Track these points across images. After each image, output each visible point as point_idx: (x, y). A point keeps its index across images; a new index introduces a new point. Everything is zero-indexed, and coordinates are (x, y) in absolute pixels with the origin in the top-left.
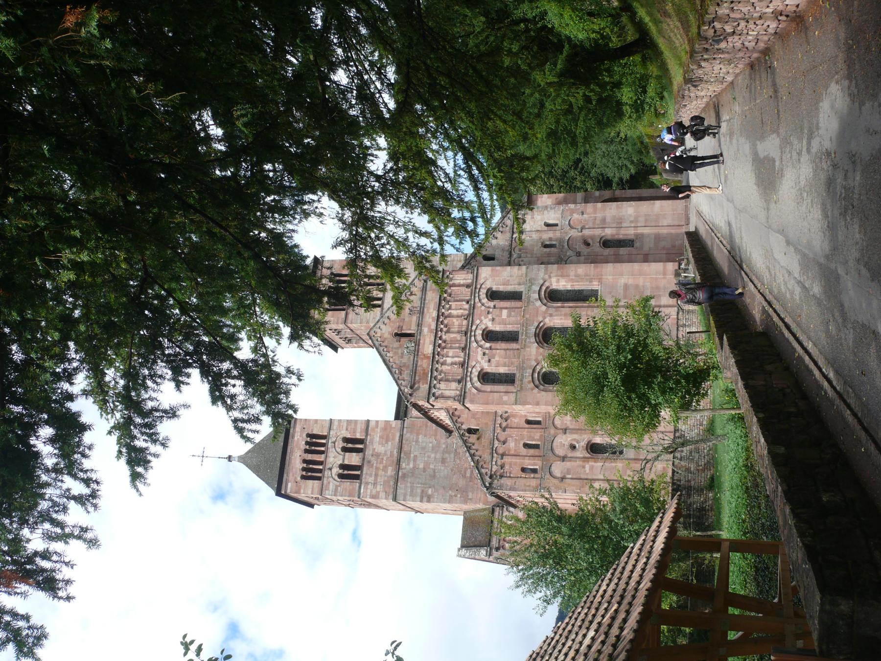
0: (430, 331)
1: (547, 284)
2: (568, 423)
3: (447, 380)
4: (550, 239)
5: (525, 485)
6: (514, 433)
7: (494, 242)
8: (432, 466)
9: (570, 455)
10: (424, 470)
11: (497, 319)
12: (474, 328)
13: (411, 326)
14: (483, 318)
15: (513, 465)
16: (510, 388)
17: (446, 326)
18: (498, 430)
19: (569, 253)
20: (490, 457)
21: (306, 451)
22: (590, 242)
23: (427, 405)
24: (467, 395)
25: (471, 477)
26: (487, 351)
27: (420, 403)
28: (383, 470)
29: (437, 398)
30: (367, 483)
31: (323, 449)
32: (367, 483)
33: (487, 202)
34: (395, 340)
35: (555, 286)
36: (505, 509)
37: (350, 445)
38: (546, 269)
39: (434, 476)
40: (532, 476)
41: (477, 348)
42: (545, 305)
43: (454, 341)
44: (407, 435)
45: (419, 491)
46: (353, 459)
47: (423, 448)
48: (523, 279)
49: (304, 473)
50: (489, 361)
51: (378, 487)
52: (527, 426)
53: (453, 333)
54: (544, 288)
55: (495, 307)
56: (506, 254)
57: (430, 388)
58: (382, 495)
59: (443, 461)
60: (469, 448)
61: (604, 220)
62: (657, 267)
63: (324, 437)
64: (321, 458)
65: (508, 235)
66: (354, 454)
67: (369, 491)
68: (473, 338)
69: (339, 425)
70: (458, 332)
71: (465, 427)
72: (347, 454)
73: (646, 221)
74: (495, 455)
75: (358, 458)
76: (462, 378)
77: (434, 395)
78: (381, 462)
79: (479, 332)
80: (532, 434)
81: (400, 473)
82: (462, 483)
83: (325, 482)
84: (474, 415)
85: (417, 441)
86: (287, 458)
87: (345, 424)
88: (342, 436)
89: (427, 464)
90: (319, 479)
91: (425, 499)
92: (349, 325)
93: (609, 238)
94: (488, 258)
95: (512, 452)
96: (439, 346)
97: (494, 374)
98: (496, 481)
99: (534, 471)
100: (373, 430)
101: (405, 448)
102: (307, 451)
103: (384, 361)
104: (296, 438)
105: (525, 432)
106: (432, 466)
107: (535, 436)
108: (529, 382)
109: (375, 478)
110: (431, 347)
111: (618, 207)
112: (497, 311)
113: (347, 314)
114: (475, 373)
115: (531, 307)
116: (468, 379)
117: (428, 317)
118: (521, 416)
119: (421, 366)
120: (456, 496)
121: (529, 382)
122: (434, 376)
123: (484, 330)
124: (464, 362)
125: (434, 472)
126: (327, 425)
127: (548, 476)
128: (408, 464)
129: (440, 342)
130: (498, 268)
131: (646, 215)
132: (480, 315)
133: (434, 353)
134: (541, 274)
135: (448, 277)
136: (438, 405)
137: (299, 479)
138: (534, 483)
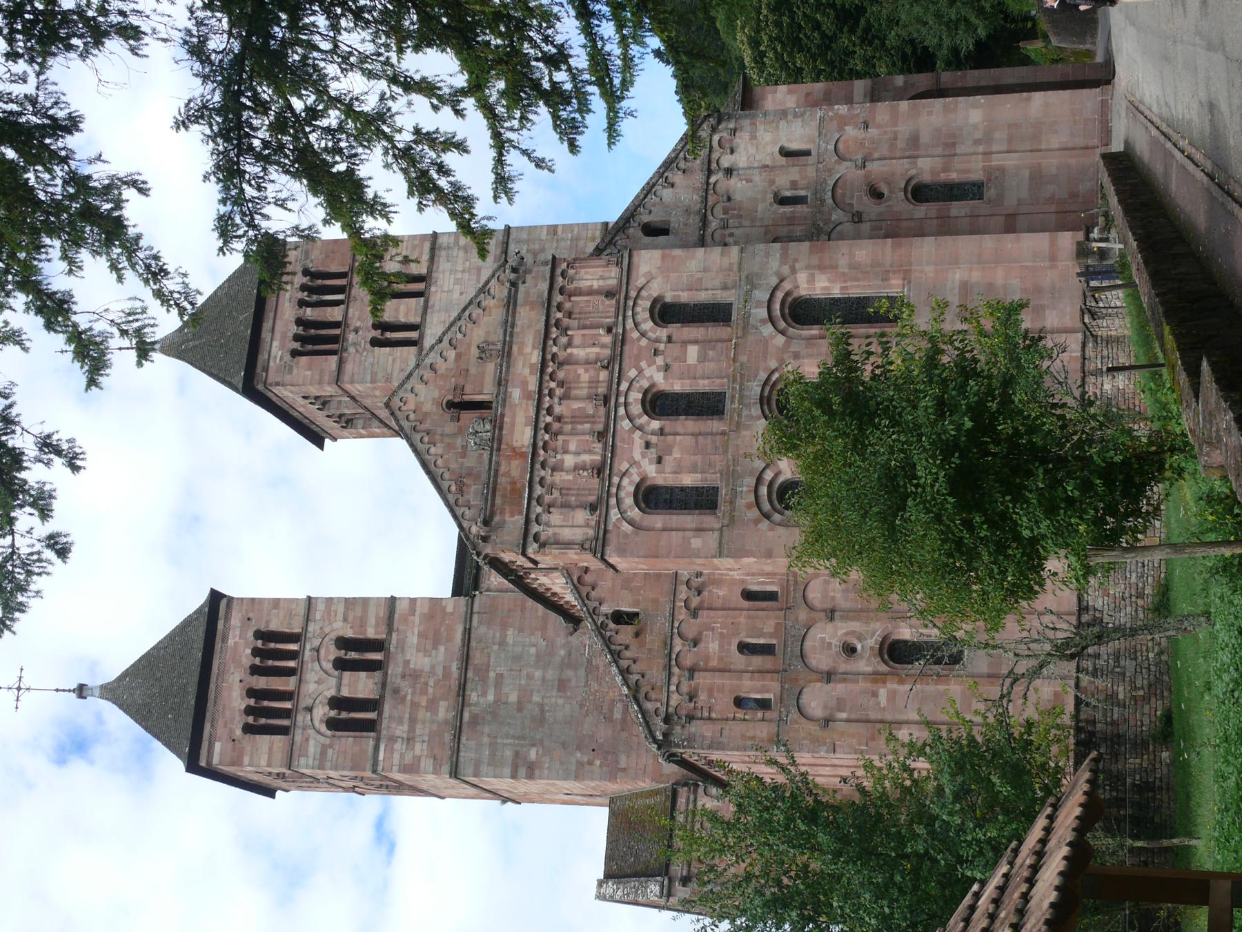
0: (527, 395)
1: (787, 286)
2: (839, 595)
3: (566, 505)
4: (794, 185)
5: (743, 736)
6: (718, 620)
7: (667, 194)
9: (844, 666)
10: (520, 707)
11: (675, 367)
12: (624, 386)
13: (482, 385)
14: (643, 364)
15: (715, 692)
16: (708, 520)
17: (561, 384)
18: (682, 614)
19: (837, 215)
20: (664, 675)
21: (255, 670)
22: (885, 190)
23: (521, 561)
24: (612, 537)
25: (624, 720)
26: (654, 439)
27: (507, 557)
28: (427, 709)
29: (543, 545)
30: (392, 739)
31: (292, 664)
32: (392, 739)
33: (613, 48)
34: (447, 416)
35: (804, 290)
36: (701, 791)
37: (353, 655)
38: (785, 254)
39: (540, 720)
40: (760, 715)
41: (631, 431)
42: (783, 333)
43: (578, 418)
44: (480, 630)
45: (509, 753)
46: (361, 685)
47: (517, 658)
48: (733, 277)
49: (250, 719)
50: (659, 460)
51: (418, 747)
52: (746, 604)
53: (577, 399)
54: (780, 295)
55: (670, 339)
56: (695, 221)
58: (427, 764)
59: (562, 685)
60: (616, 656)
61: (914, 141)
62: (1032, 243)
63: (294, 638)
64: (289, 684)
65: (699, 178)
66: (363, 674)
67: (396, 756)
68: (622, 411)
70: (589, 398)
71: (606, 609)
72: (347, 674)
73: (1010, 139)
74: (676, 670)
75: (370, 683)
76: (600, 499)
77: (536, 538)
79: (636, 396)
80: (759, 624)
81: (466, 716)
82: (604, 733)
83: (298, 738)
84: (627, 582)
85: (502, 643)
86: (212, 686)
87: (341, 609)
88: (334, 635)
89: (525, 694)
90: (284, 731)
91: (522, 771)
92: (348, 387)
93: (927, 178)
94: (655, 231)
95: (714, 663)
96: (547, 428)
97: (671, 490)
98: (678, 729)
99: (764, 704)
100: (406, 620)
101: (477, 658)
102: (255, 670)
103: (424, 465)
104: (231, 642)
105: (742, 619)
107: (764, 627)
108: (749, 506)
109: (408, 729)
110: (529, 432)
111: (946, 109)
112: (674, 350)
113: (341, 363)
114: (628, 487)
115: (751, 338)
116: (613, 501)
117: (521, 363)
118: (733, 582)
119: (507, 474)
120: (590, 763)
121: (749, 506)
122: (534, 497)
124: (604, 462)
125: (542, 711)
126: (302, 611)
127: (794, 714)
128: (484, 694)
129: (549, 419)
130: (678, 252)
131: (1010, 126)
132: (638, 359)
133: (535, 445)
134: (774, 264)
135: (563, 274)
136: (545, 560)
137: (239, 732)
138: (763, 731)
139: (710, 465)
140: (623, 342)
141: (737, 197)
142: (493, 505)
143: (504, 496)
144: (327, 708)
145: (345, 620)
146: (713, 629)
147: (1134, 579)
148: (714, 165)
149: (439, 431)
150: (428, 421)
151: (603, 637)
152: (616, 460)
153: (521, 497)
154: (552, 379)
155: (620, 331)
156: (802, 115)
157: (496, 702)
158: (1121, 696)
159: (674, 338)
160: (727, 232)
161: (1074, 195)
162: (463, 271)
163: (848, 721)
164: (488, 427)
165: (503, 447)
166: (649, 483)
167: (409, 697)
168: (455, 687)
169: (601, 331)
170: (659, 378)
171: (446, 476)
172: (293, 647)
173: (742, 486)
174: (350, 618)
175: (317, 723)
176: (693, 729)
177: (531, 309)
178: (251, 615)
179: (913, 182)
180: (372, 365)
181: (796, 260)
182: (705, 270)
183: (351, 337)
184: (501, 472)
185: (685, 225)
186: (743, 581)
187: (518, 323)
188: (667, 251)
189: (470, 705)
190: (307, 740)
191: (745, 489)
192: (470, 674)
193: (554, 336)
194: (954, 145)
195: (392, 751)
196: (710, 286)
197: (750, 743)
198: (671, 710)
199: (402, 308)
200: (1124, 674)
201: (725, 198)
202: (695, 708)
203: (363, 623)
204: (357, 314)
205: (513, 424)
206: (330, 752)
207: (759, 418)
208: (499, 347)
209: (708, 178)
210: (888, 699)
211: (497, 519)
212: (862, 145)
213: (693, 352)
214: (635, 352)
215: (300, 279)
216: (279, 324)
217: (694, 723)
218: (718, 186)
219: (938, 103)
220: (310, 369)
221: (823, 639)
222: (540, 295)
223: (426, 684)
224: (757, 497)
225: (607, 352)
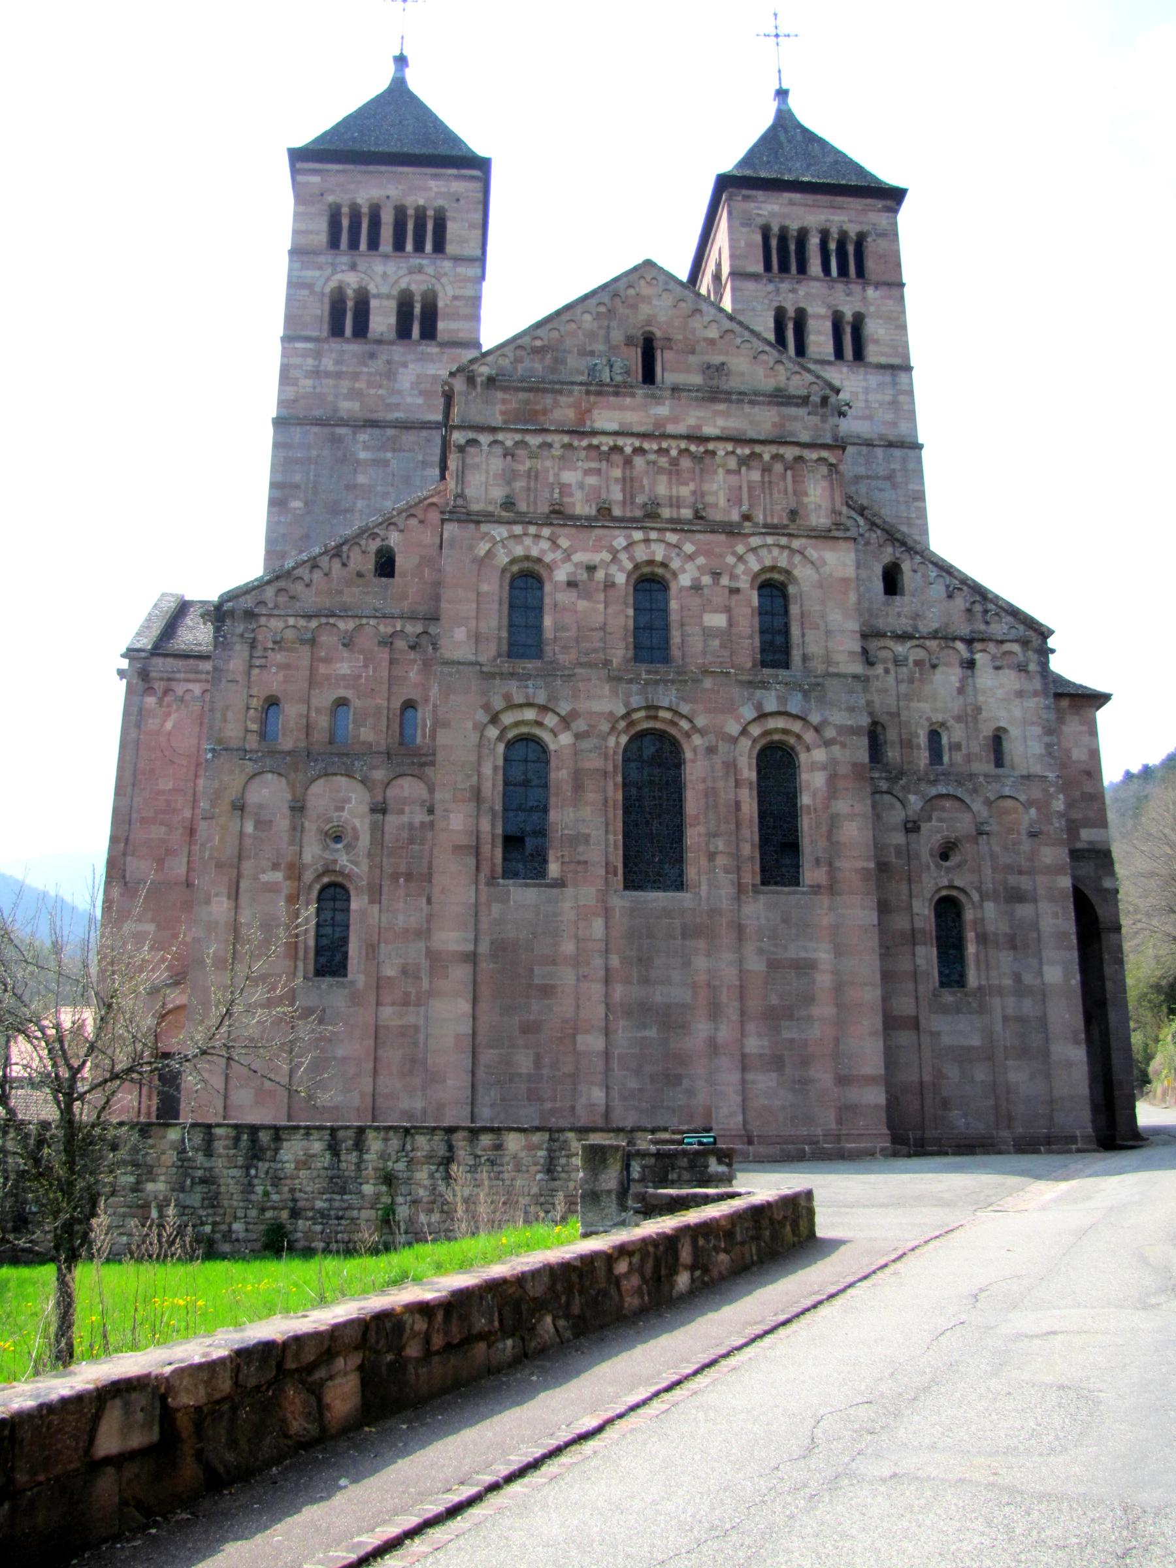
0: (660, 423)
1: (809, 736)
5: (227, 708)
7: (938, 590)
8: (360, 504)
12: (672, 538)
14: (701, 560)
17: (674, 462)
18: (385, 629)
26: (600, 575)
28: (352, 389)
30: (318, 355)
32: (318, 355)
38: (854, 731)
39: (335, 510)
42: (744, 732)
45: (297, 478)
46: (382, 320)
52: (397, 704)
54: (796, 727)
55: (735, 591)
56: (904, 624)
57: (493, 430)
58: (291, 392)
60: (336, 553)
62: (868, 1053)
63: (439, 247)
65: (964, 630)
66: (393, 320)
68: (638, 535)
69: (466, 280)
71: (394, 539)
78: (370, 385)
81: (342, 431)
83: (322, 259)
86: (383, 168)
87: (469, 292)
88: (438, 287)
90: (334, 243)
93: (969, 915)
94: (892, 582)
95: (322, 669)
98: (240, 628)
101: (409, 438)
103: (568, 308)
104: (432, 183)
106: (360, 504)
108: (507, 697)
110: (613, 426)
112: (720, 598)
113: (754, 277)
115: (735, 691)
116: (518, 529)
117: (700, 413)
119: (556, 404)
121: (507, 697)
123: (664, 565)
125: (347, 511)
127: (250, 767)
128: (366, 448)
130: (853, 597)
132: (708, 553)
133: (594, 433)
134: (839, 718)
137: (330, 199)
139: (565, 647)
140: (730, 534)
141: (938, 676)
142: (518, 389)
143: (527, 402)
144: (355, 286)
145: (455, 298)
146: (366, 666)
147: (319, 1204)
148: (978, 646)
149: (614, 324)
150: (627, 311)
151: (359, 535)
152: (573, 531)
153: (526, 422)
154: (682, 452)
155: (746, 531)
156: (1050, 754)
157: (358, 461)
158: (150, 1186)
159: (735, 597)
160: (891, 666)
161: (946, 1104)
162: (867, 401)
163: (241, 834)
164: (619, 378)
165: (592, 398)
166: (544, 573)
167: (365, 370)
168: (375, 416)
169: (745, 508)
170: (685, 580)
171: (555, 334)
172: (429, 247)
173: (535, 687)
174: (457, 303)
175: (338, 277)
176: (238, 647)
177: (774, 425)
178: (462, 202)
179: (962, 898)
180: (753, 309)
181: (843, 746)
182: (828, 633)
183: (785, 286)
184: (559, 397)
185: (899, 614)
186: (427, 701)
187: (757, 409)
188: (853, 585)
189: (354, 433)
190: (320, 268)
191: (531, 691)
192: (390, 432)
193: (739, 451)
194: (1014, 947)
195: (304, 356)
196: (807, 639)
197: (218, 715)
198: (263, 620)
199: (822, 338)
200: (182, 1189)
201: (935, 661)
202: (266, 649)
203: (455, 316)
204: (814, 291)
205: (622, 408)
206: (306, 292)
207: (626, 704)
208: (725, 387)
209: (962, 640)
210: (268, 883)
211: (500, 395)
212: (1010, 831)
213: (718, 620)
214: (717, 550)
215: (853, 230)
216: (798, 211)
217: (246, 647)
218: (951, 652)
219: (1070, 927)
220: (747, 245)
221: (348, 800)
222: (792, 434)
223: (380, 386)
224: (521, 706)
225: (718, 517)
